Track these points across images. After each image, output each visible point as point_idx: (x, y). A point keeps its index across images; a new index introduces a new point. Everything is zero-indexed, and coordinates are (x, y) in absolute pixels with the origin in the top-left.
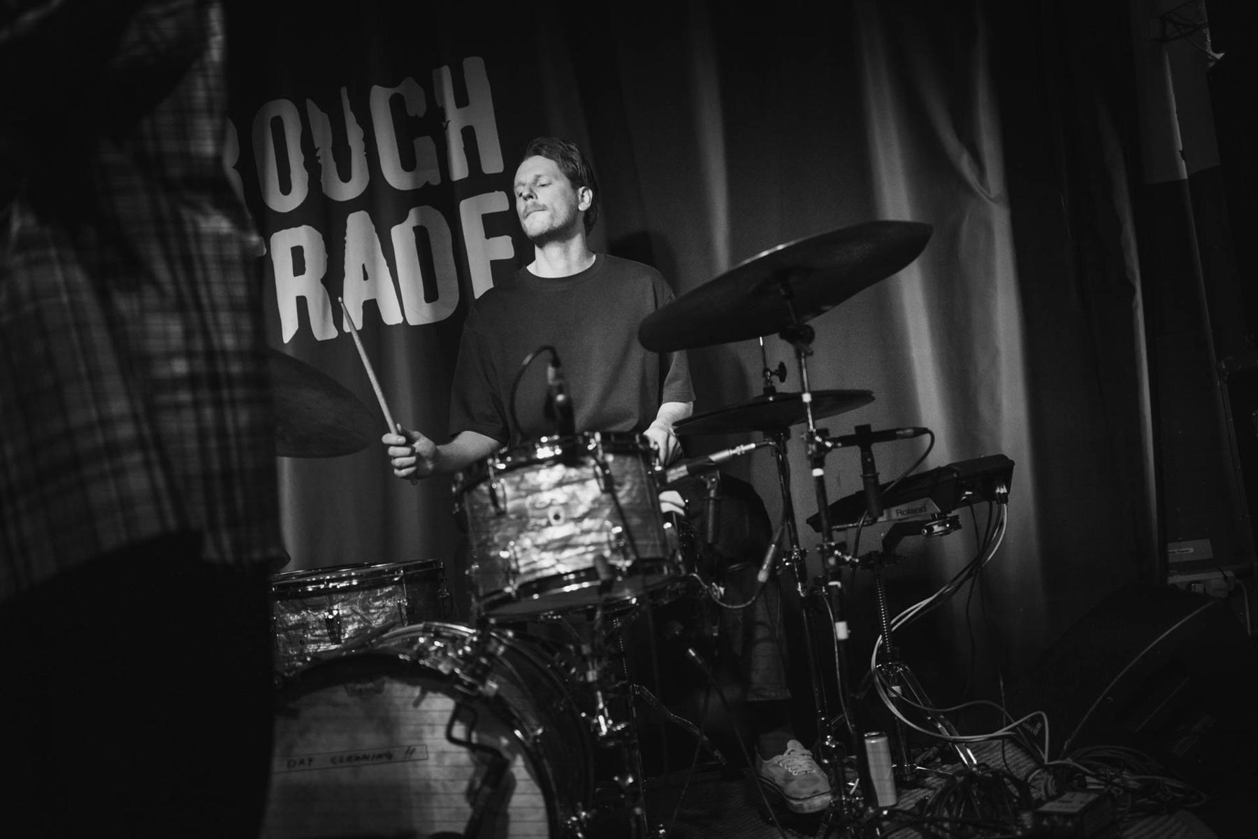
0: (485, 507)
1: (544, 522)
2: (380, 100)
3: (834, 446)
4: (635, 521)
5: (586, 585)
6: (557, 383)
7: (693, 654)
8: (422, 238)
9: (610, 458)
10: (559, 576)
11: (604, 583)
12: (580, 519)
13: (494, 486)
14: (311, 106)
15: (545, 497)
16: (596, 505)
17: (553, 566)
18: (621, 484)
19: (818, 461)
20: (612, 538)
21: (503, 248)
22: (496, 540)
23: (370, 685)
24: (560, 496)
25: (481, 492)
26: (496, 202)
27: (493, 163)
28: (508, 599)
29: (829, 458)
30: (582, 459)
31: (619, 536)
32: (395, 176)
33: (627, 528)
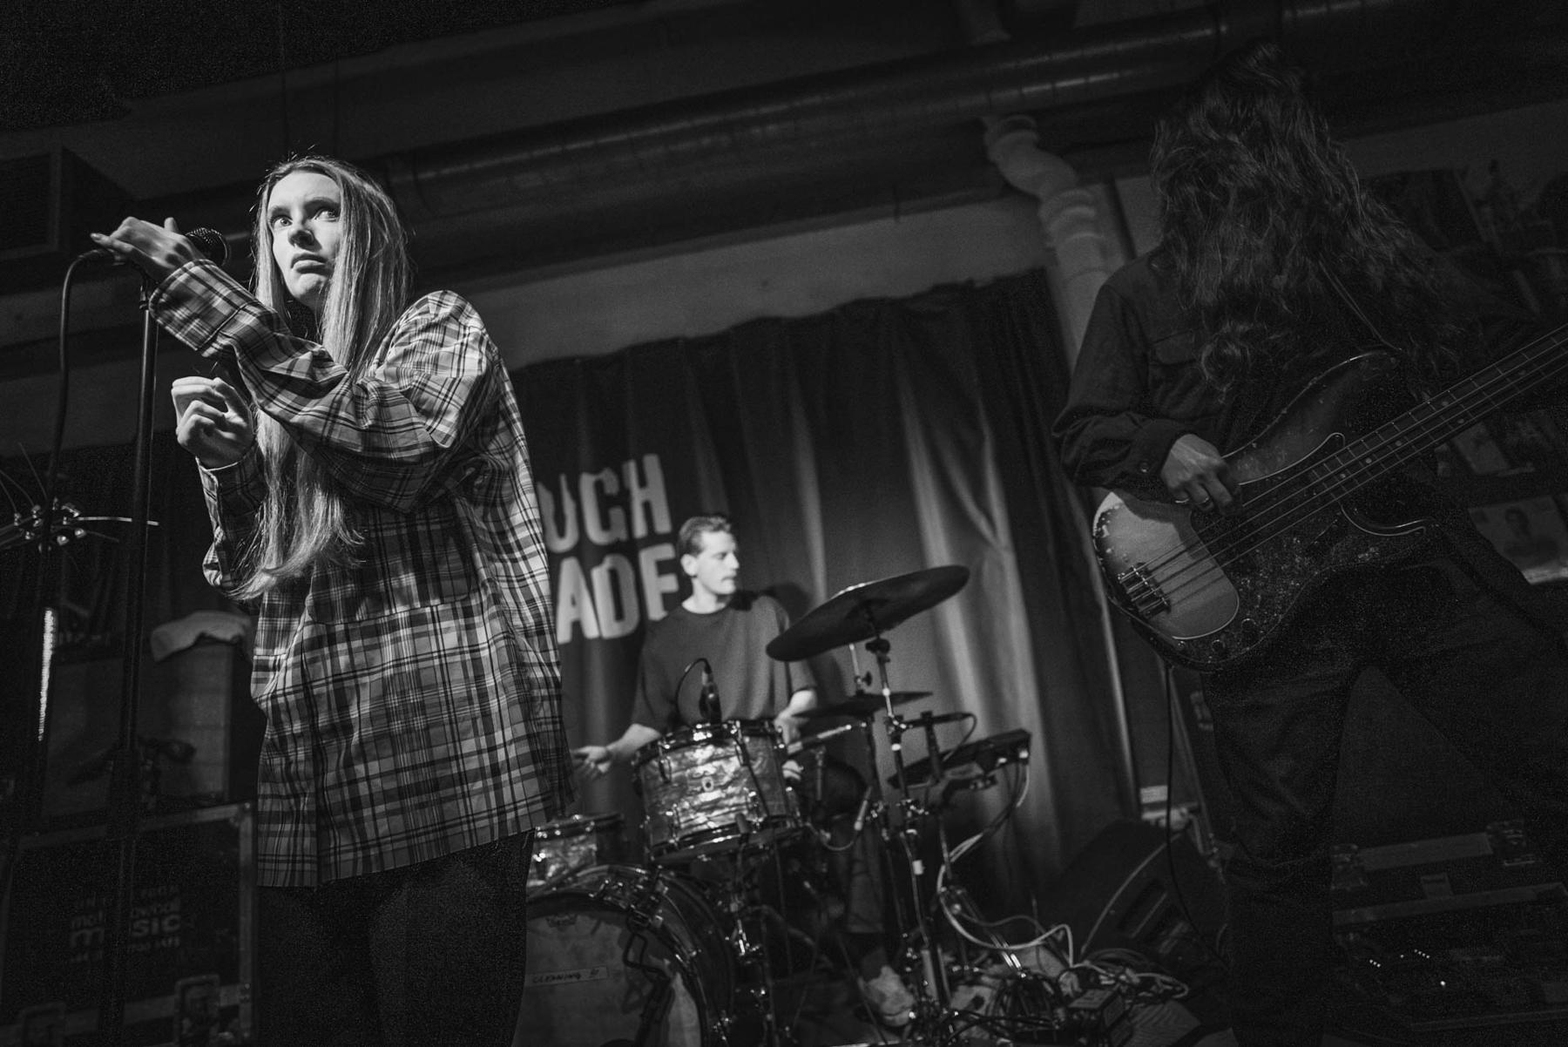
0: (655, 778)
1: (698, 789)
2: (587, 482)
3: (907, 728)
4: (765, 787)
5: (729, 837)
6: (708, 685)
9: (747, 740)
10: (710, 830)
11: (743, 835)
12: (724, 787)
13: (662, 762)
15: (700, 770)
16: (737, 776)
17: (705, 823)
18: (755, 759)
19: (896, 739)
20: (749, 800)
21: (670, 583)
22: (663, 803)
23: (567, 917)
24: (710, 769)
25: (654, 767)
26: (666, 552)
27: (663, 525)
28: (671, 848)
29: (904, 736)
30: (726, 741)
31: (754, 799)
32: (596, 535)
33: (760, 793)
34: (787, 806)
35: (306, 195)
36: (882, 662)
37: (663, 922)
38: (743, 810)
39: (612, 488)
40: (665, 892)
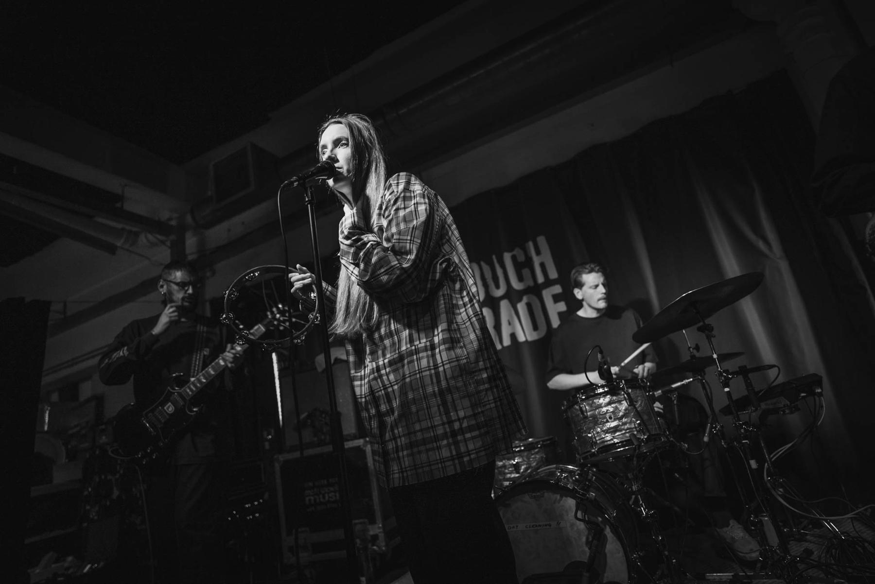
0: (578, 415)
1: (605, 420)
2: (507, 257)
4: (645, 417)
6: (603, 360)
7: (678, 476)
8: (529, 307)
10: (615, 444)
12: (620, 419)
14: (483, 264)
17: (612, 440)
18: (637, 402)
21: (562, 307)
23: (538, 494)
24: (610, 409)
26: (557, 289)
27: (553, 274)
28: (593, 455)
32: (516, 285)
33: (642, 420)
34: (660, 428)
35: (333, 137)
36: (709, 338)
37: (595, 496)
38: (634, 431)
39: (521, 258)
40: (594, 479)
